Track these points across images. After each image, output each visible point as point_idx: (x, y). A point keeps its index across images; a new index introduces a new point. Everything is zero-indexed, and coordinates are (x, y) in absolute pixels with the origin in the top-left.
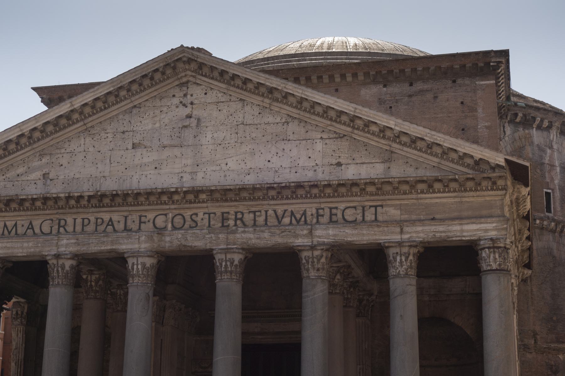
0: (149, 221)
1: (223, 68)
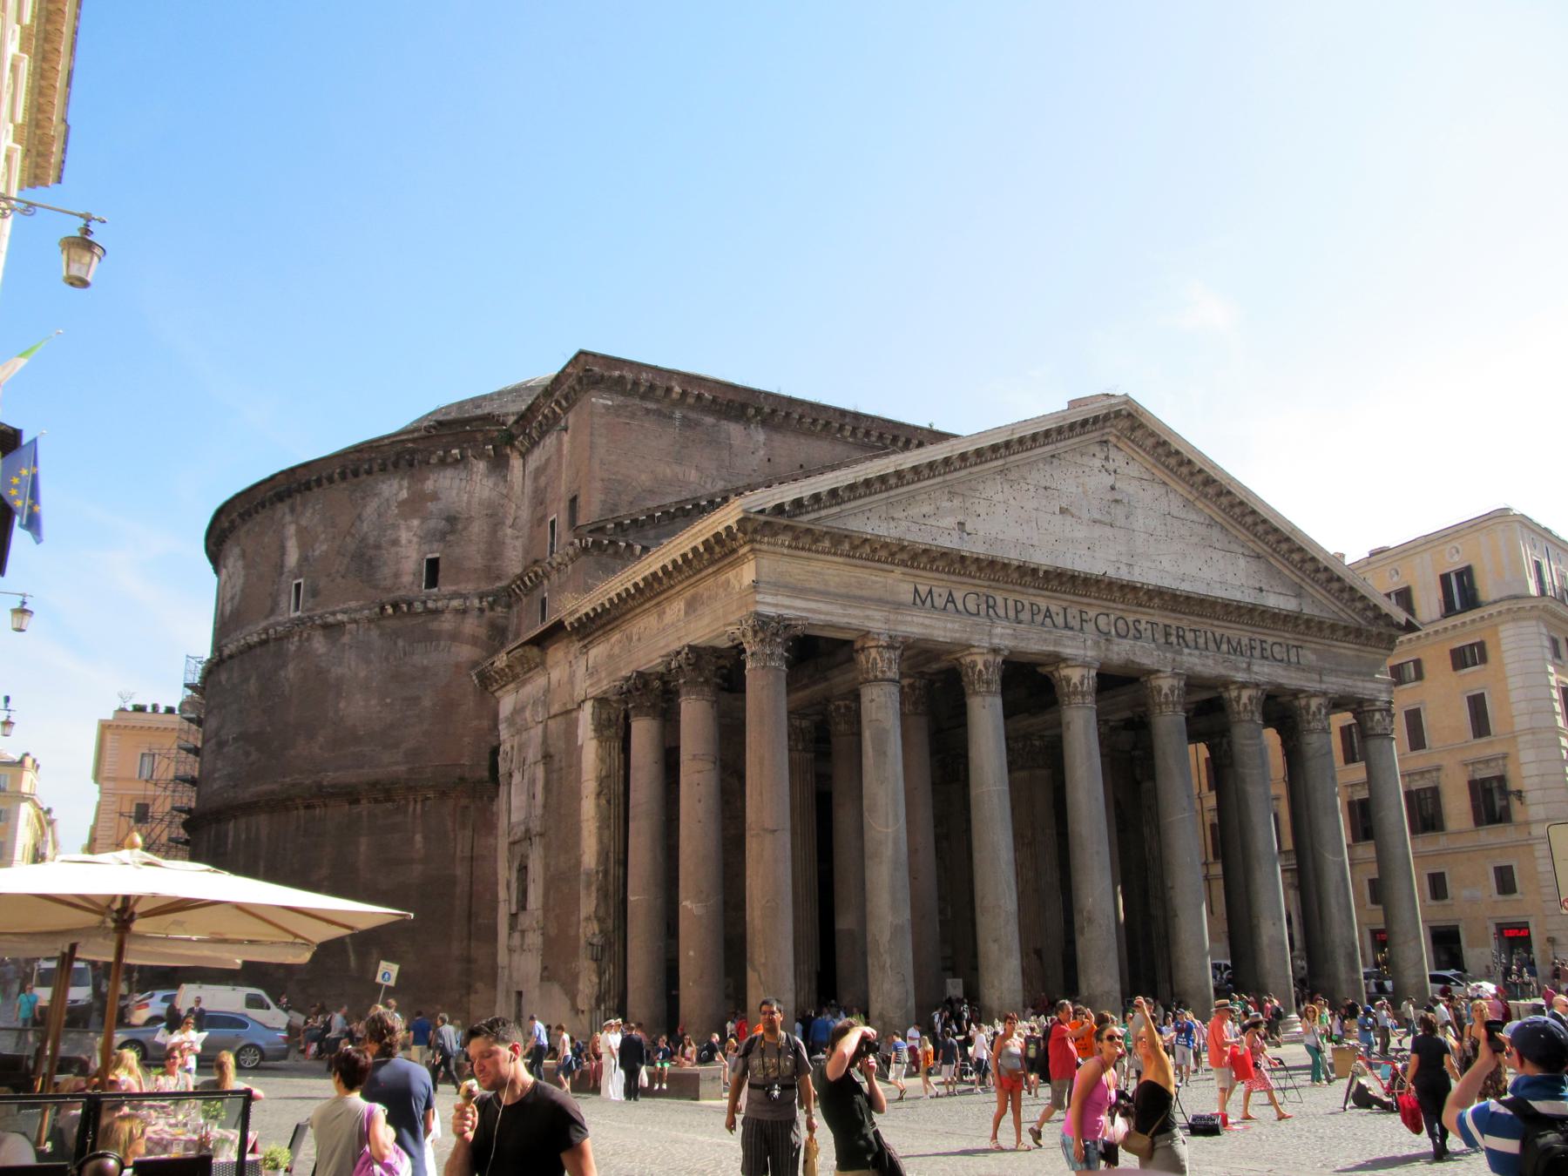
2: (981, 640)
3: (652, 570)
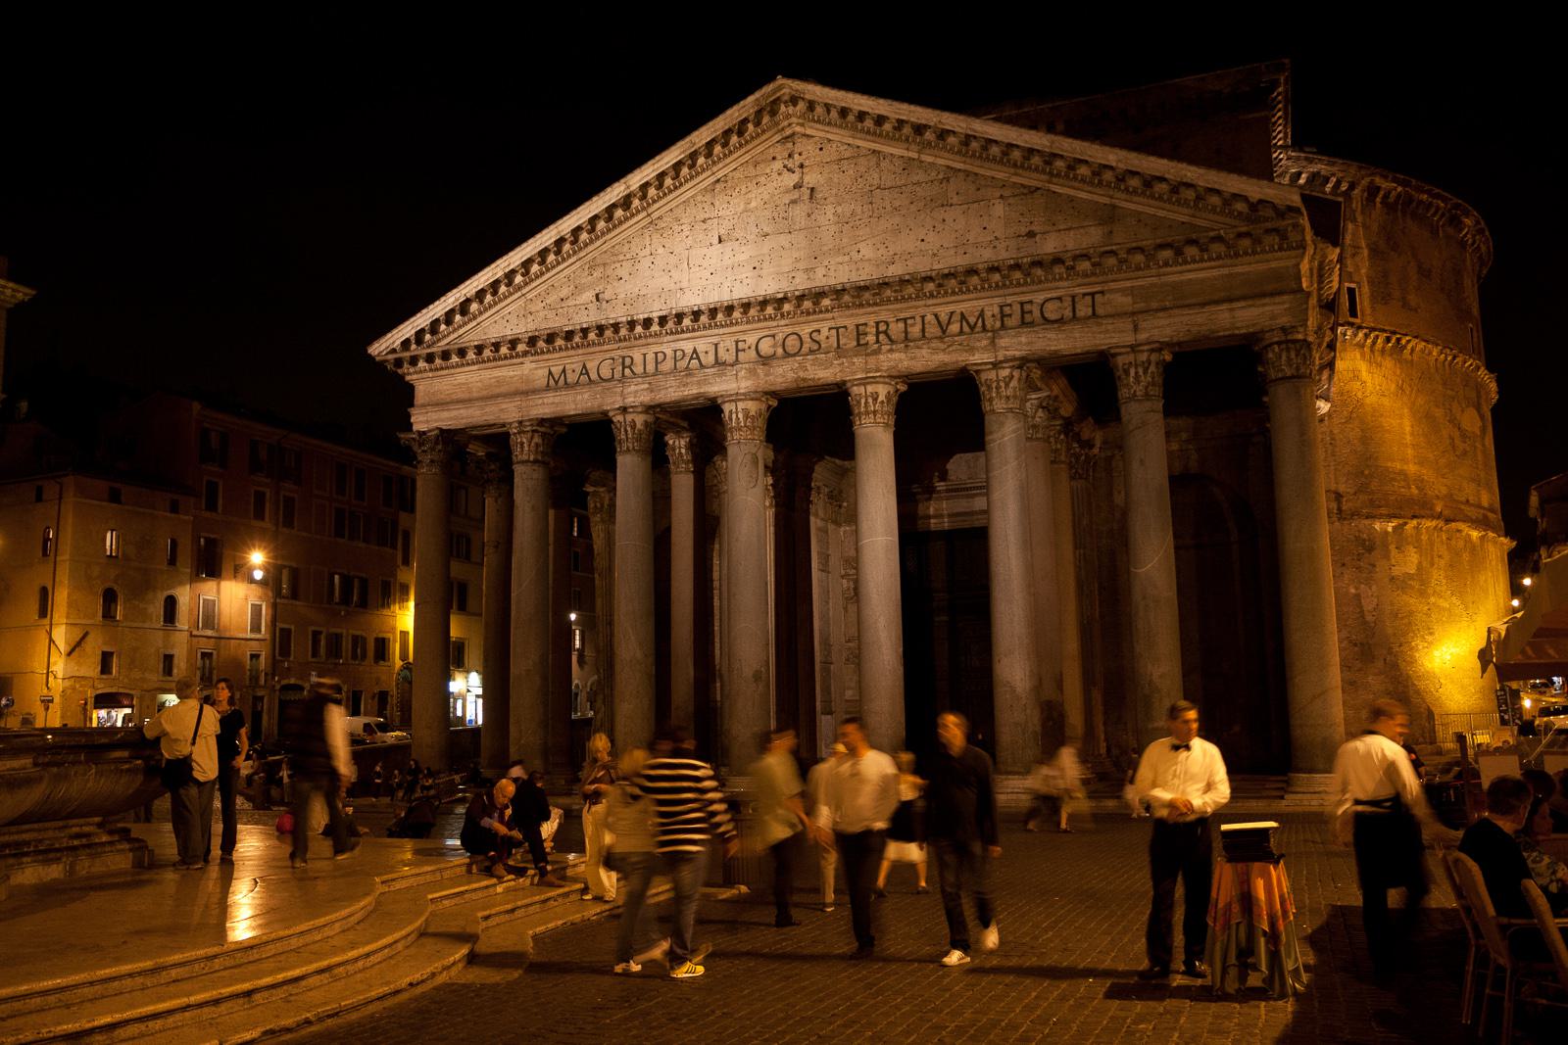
0: (749, 348)
1: (843, 105)
2: (610, 402)
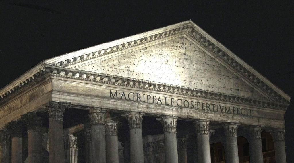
3: (17, 85)
